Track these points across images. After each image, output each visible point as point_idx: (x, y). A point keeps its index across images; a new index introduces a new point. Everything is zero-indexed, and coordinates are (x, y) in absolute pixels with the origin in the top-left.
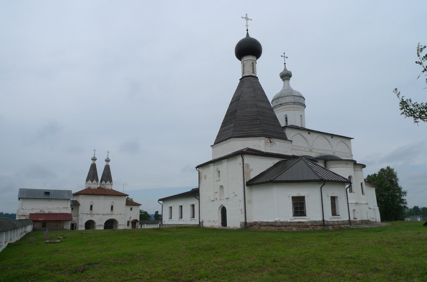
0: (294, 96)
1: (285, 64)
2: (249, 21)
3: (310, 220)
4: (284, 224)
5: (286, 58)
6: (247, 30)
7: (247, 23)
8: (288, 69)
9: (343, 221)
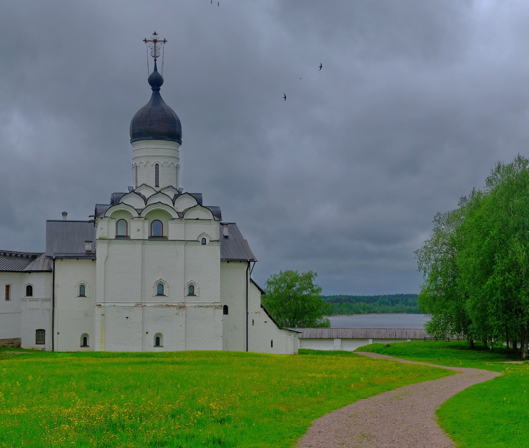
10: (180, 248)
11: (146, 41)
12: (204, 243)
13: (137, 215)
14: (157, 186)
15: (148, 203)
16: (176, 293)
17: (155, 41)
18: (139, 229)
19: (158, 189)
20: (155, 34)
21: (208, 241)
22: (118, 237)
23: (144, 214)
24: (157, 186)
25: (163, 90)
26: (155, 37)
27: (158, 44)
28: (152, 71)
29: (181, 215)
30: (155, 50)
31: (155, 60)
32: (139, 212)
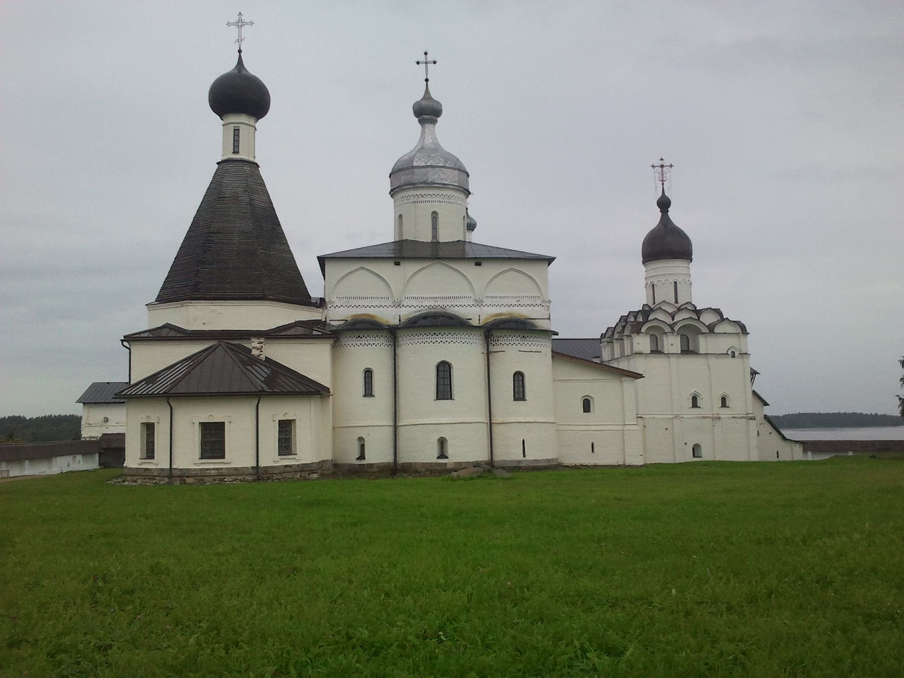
0: (413, 167)
1: (427, 80)
2: (245, 29)
3: (159, 467)
4: (132, 472)
5: (430, 66)
6: (240, 51)
7: (240, 34)
8: (435, 95)
9: (236, 469)
10: (712, 361)
11: (653, 166)
12: (733, 356)
13: (670, 330)
14: (676, 302)
16: (710, 405)
17: (662, 166)
18: (672, 343)
19: (678, 305)
21: (737, 354)
22: (652, 352)
23: (676, 328)
24: (676, 302)
25: (672, 213)
26: (661, 163)
27: (665, 169)
28: (661, 194)
29: (711, 328)
32: (672, 327)
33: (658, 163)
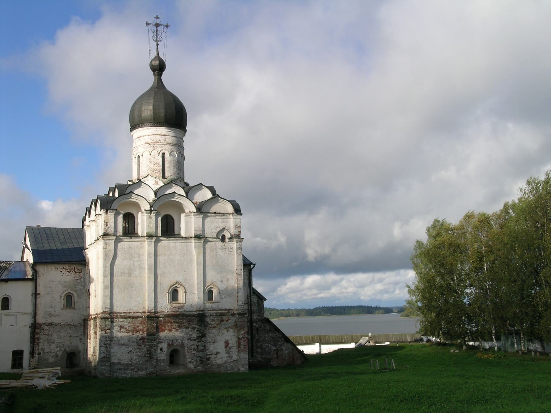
15: (158, 196)
17: (157, 25)
20: (157, 18)
24: (163, 177)
25: (164, 77)
26: (157, 21)
27: (160, 28)
28: (154, 55)
30: (157, 34)
31: (158, 45)
33: (152, 20)
